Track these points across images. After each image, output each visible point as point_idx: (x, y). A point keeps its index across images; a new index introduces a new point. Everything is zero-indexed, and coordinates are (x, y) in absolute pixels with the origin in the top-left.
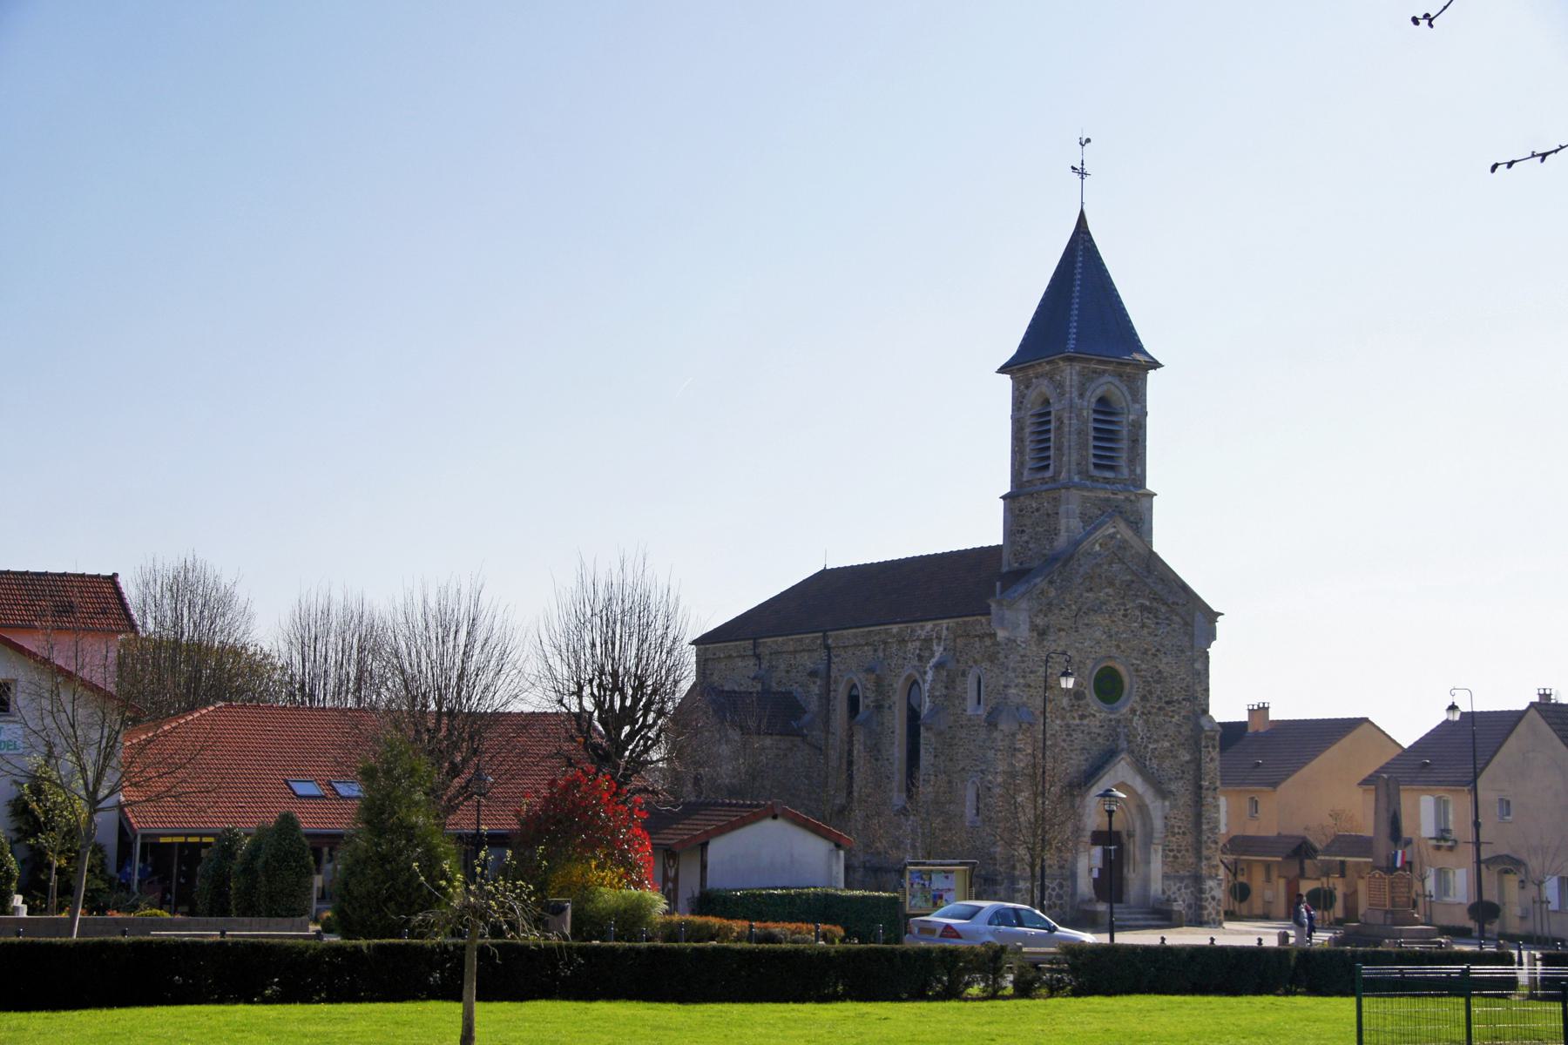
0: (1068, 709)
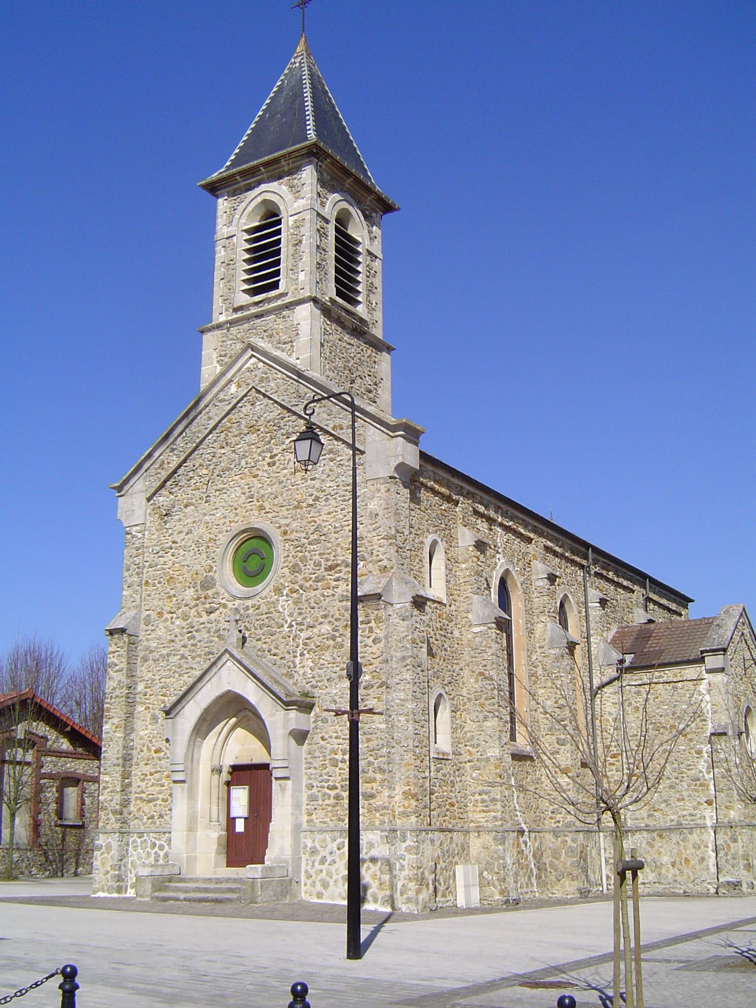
0: (193, 603)
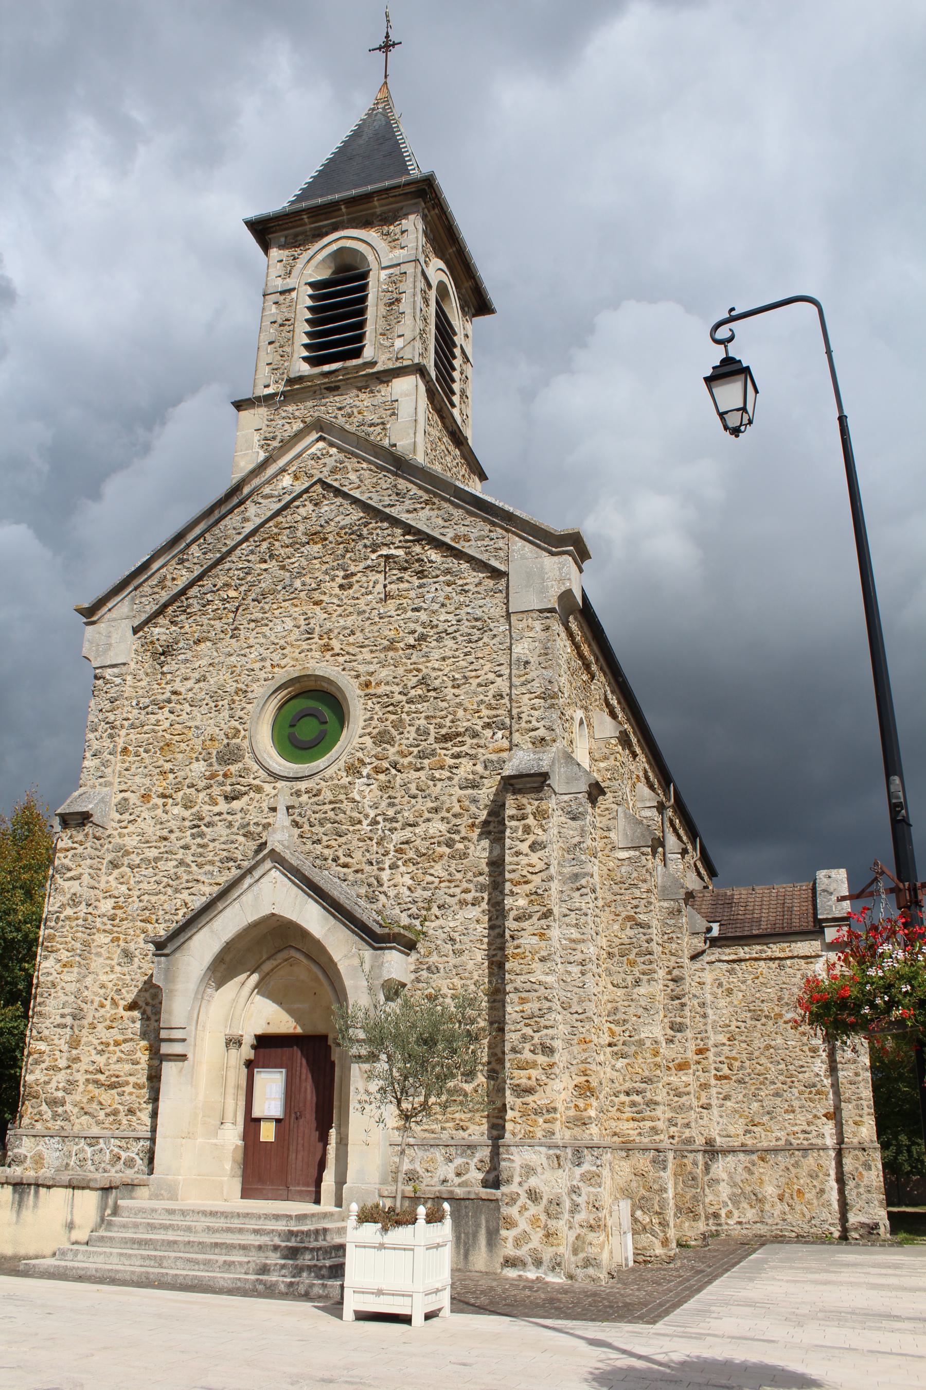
0: (202, 784)
